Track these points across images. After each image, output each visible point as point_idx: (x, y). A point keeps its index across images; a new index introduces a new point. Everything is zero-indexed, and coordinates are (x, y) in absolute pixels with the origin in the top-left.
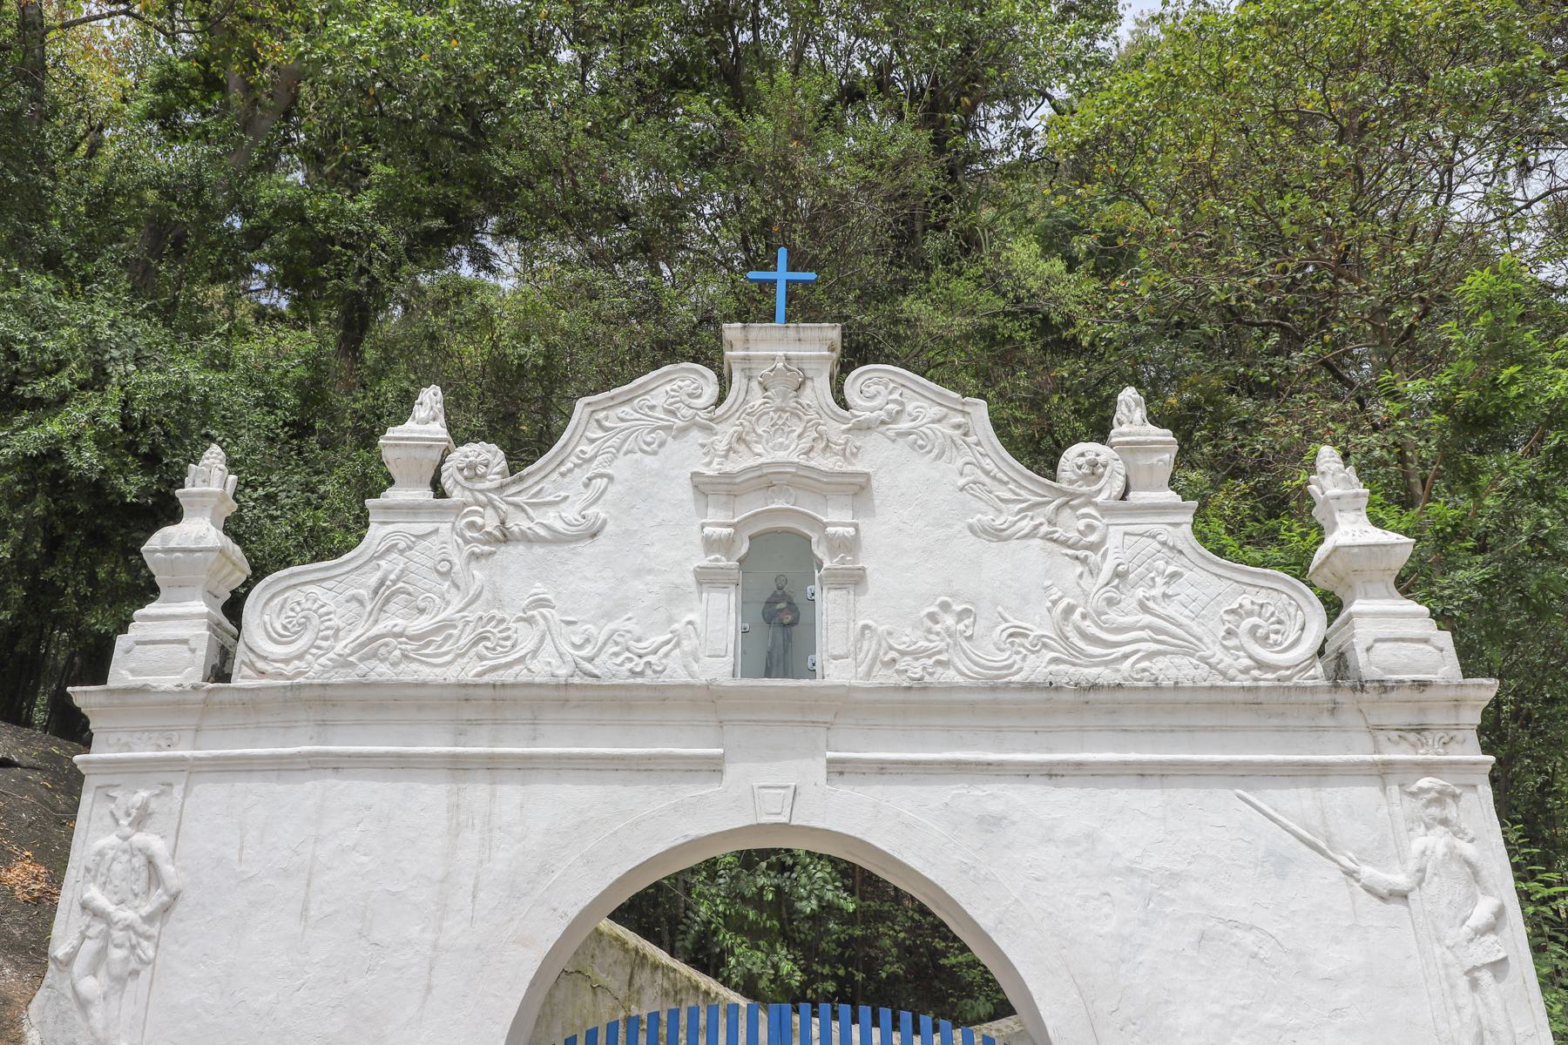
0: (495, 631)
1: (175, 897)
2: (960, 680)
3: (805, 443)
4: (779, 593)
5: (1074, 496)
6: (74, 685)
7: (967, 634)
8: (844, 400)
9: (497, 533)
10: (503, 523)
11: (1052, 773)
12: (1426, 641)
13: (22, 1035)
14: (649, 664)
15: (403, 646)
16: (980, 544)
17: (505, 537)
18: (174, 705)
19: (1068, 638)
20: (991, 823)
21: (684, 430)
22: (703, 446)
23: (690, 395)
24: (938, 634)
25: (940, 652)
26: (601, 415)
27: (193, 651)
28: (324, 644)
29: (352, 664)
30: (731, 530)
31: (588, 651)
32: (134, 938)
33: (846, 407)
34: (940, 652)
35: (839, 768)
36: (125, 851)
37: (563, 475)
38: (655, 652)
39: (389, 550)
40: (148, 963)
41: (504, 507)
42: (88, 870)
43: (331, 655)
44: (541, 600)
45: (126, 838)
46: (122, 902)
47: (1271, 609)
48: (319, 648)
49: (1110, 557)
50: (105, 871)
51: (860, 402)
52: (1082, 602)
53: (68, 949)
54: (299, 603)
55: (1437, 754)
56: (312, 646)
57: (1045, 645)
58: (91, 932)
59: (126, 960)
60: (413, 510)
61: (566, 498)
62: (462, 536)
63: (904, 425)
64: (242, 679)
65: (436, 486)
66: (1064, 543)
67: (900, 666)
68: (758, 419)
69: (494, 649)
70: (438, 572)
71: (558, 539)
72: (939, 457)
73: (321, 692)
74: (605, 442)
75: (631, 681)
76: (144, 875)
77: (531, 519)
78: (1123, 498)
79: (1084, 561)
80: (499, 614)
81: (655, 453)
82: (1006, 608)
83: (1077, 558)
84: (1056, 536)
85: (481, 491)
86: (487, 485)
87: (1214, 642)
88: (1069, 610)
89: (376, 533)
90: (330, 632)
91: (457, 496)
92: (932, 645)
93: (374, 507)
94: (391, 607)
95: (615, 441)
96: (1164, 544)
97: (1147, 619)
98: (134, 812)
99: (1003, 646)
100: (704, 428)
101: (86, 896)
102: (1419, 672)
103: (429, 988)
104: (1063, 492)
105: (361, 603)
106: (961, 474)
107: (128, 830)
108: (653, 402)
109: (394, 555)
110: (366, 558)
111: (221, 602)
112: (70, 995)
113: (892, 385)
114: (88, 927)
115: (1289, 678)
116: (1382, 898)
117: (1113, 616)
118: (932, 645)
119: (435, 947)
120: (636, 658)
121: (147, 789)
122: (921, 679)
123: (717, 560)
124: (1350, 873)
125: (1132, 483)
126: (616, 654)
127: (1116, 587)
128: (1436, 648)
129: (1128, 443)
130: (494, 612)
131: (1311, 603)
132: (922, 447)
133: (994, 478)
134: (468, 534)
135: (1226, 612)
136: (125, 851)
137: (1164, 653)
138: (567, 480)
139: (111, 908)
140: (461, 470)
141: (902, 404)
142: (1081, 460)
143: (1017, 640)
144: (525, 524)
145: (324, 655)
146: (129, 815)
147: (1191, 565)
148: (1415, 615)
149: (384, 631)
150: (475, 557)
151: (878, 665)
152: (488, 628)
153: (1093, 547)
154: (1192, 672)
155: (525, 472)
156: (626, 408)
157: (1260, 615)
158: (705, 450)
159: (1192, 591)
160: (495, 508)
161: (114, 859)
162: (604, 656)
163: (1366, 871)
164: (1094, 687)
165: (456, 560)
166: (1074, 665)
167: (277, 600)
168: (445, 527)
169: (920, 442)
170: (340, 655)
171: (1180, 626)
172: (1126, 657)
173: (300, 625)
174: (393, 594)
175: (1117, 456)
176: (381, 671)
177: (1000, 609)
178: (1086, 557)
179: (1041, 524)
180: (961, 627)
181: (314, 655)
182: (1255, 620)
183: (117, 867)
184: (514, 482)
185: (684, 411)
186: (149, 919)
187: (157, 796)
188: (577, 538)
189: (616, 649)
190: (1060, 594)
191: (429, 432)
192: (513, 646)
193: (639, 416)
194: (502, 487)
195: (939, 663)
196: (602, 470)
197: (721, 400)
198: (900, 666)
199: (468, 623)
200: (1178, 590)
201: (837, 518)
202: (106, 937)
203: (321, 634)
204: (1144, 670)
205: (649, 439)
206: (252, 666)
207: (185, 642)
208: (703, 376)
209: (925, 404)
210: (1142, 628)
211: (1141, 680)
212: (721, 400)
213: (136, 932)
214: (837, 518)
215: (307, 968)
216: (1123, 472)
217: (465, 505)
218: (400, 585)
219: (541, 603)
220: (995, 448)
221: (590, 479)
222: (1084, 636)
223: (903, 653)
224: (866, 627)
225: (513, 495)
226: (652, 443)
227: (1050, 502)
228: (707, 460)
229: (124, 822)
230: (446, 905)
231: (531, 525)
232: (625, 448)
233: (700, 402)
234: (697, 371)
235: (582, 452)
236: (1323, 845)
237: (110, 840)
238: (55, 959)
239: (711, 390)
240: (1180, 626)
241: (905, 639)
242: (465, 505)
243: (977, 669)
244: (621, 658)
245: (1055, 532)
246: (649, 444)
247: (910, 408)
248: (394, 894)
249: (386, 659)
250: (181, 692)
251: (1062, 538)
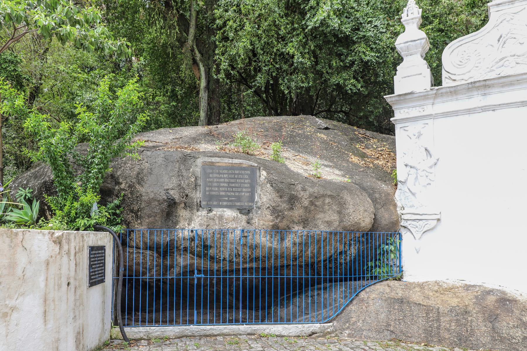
13: (396, 203)
18: (424, 97)
73: (484, 83)
93: (491, 6)
114: (410, 171)
186: (431, 167)
202: (417, 173)
250: (426, 92)
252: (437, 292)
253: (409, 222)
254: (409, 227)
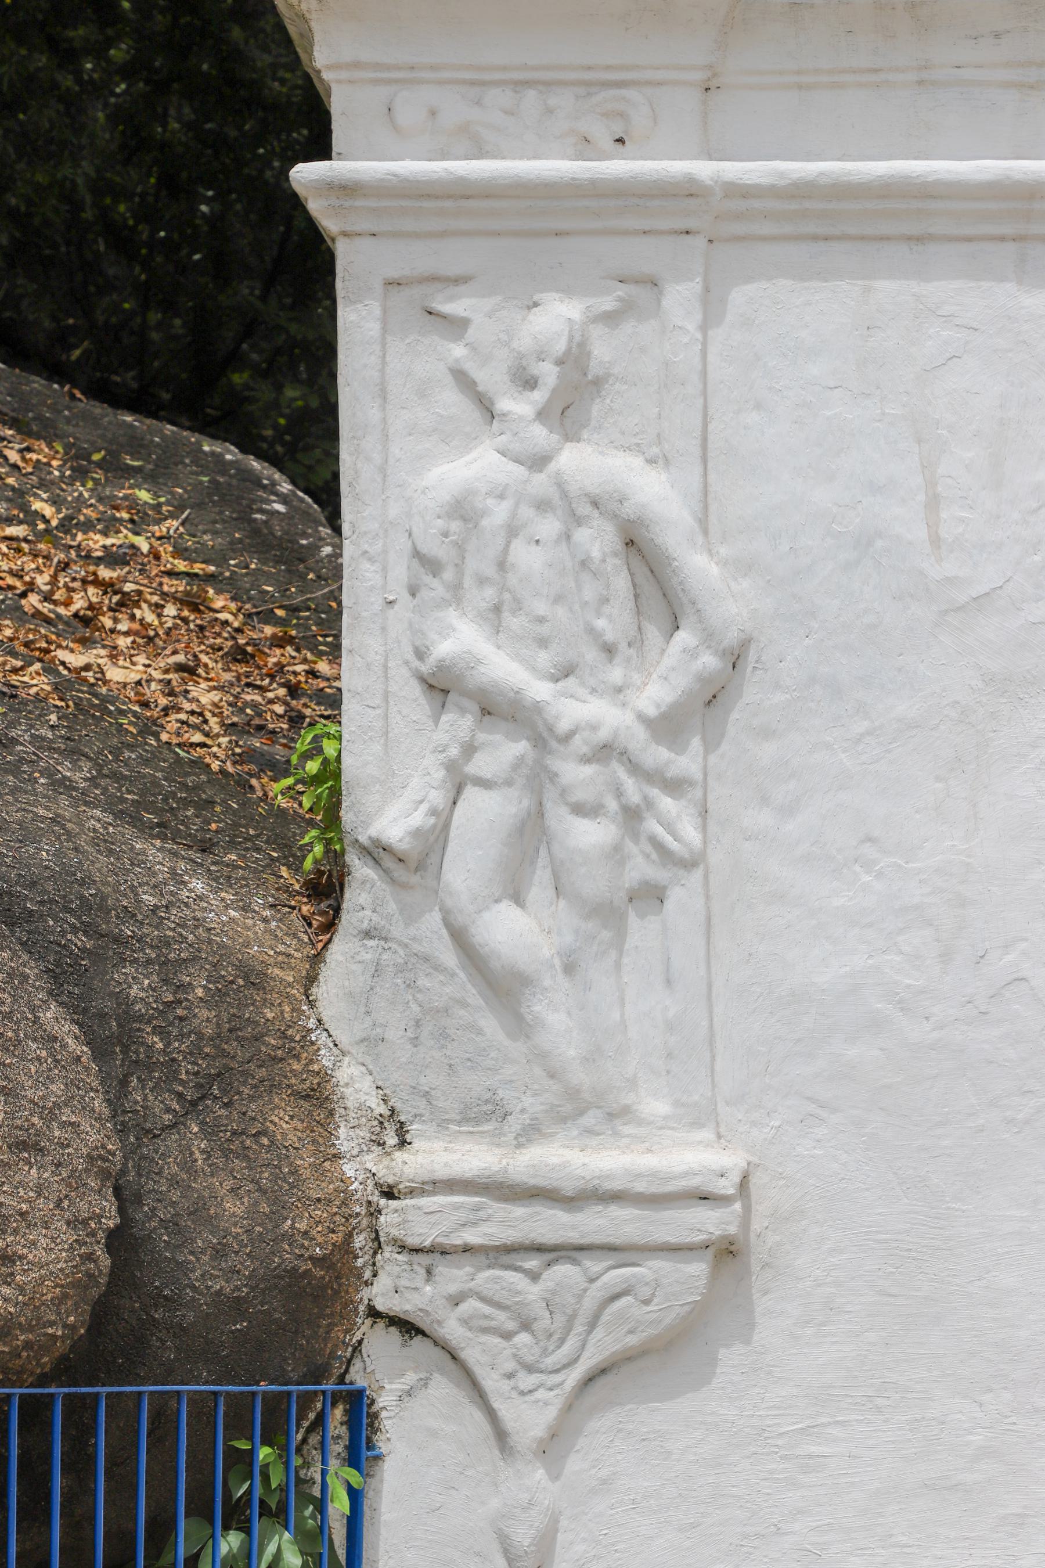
32: (633, 790)
36: (542, 506)
40: (689, 863)
42: (431, 565)
45: (538, 462)
46: (565, 672)
50: (490, 571)
53: (418, 818)
58: (482, 765)
59: (616, 854)
76: (621, 583)
98: (548, 373)
101: (444, 649)
107: (540, 435)
112: (449, 957)
121: (568, 292)
136: (542, 506)
139: (539, 690)
146: (530, 383)
161: (512, 531)
187: (610, 319)
213: (635, 768)
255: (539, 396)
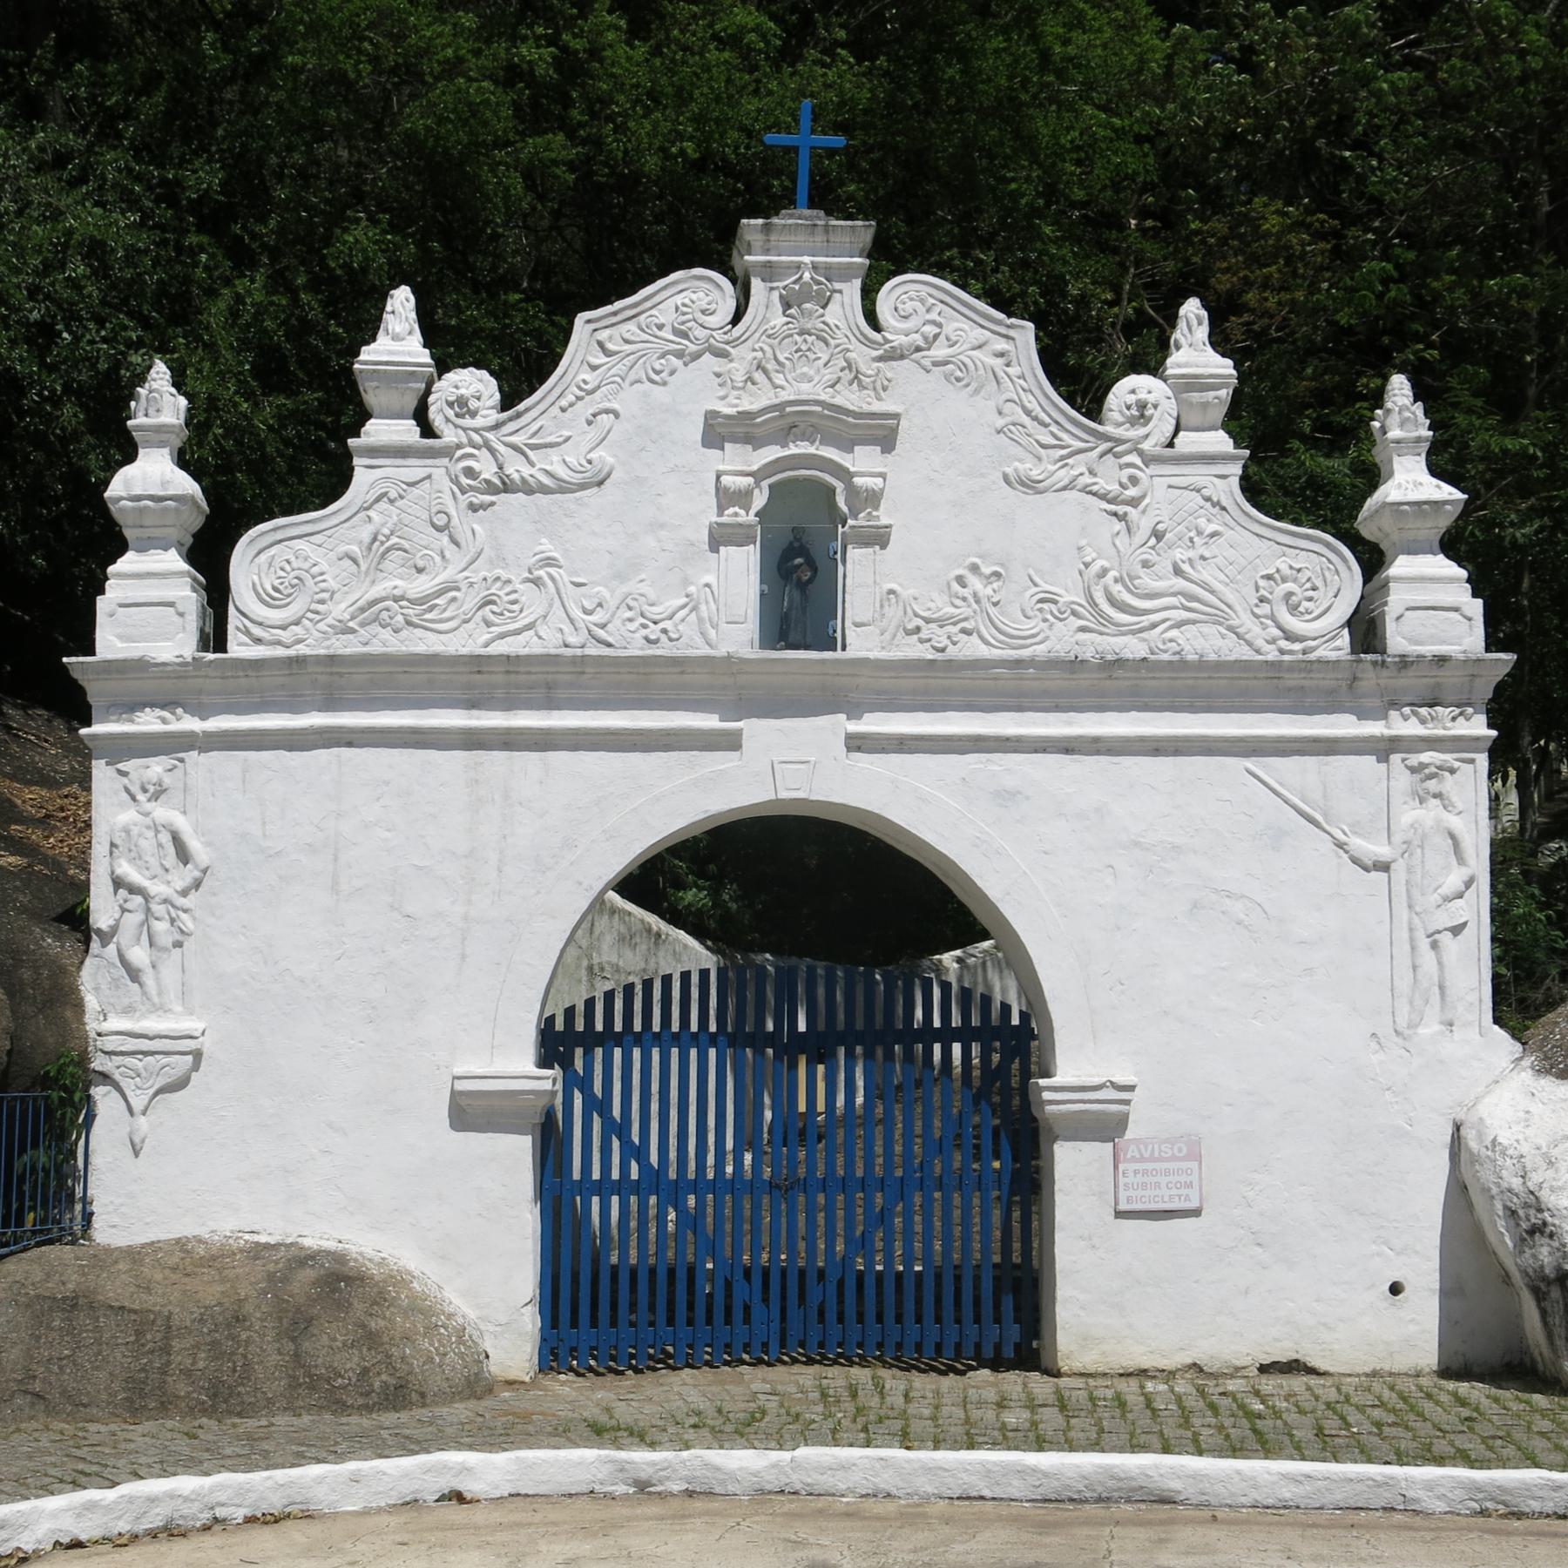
0: (501, 593)
1: (205, 871)
2: (984, 652)
3: (829, 375)
4: (796, 544)
5: (1120, 441)
6: (68, 656)
7: (994, 600)
8: (874, 311)
9: (497, 481)
10: (501, 468)
11: (1068, 747)
12: (1456, 610)
14: (665, 631)
15: (404, 611)
16: (1013, 496)
17: (507, 487)
19: (1097, 605)
20: (1006, 797)
21: (696, 356)
22: (718, 375)
23: (703, 312)
24: (964, 599)
25: (966, 619)
26: (603, 335)
27: (181, 615)
28: (320, 607)
29: (353, 631)
30: (750, 480)
31: (598, 617)
33: (876, 327)
34: (966, 619)
35: (858, 743)
36: (148, 827)
37: (563, 410)
38: (670, 618)
39: (378, 500)
41: (501, 448)
43: (330, 620)
44: (549, 558)
46: (154, 877)
47: (1308, 574)
48: (317, 613)
49: (1150, 512)
51: (893, 322)
52: (1116, 564)
53: (112, 922)
54: (288, 562)
55: (1445, 728)
56: (309, 610)
57: (1074, 613)
60: (401, 452)
61: (568, 439)
62: (457, 482)
63: (939, 352)
64: (238, 647)
65: (421, 415)
66: (1103, 497)
67: (924, 634)
68: (780, 343)
69: (502, 614)
70: (434, 525)
71: (564, 488)
72: (977, 391)
74: (610, 369)
75: (649, 652)
77: (532, 464)
78: (1171, 445)
79: (1121, 518)
80: (504, 575)
81: (665, 384)
82: (1037, 571)
83: (1115, 514)
84: (1095, 488)
85: (476, 430)
86: (478, 422)
87: (1245, 610)
88: (1104, 572)
89: (364, 478)
90: (325, 595)
91: (449, 436)
92: (957, 611)
94: (387, 565)
95: (620, 368)
96: (1208, 499)
97: (1181, 583)
99: (1030, 613)
100: (721, 354)
101: (119, 871)
102: (1443, 642)
103: (463, 957)
104: (1106, 437)
105: (355, 561)
106: (1000, 413)
108: (662, 320)
109: (383, 505)
110: (354, 510)
111: (185, 549)
113: (932, 301)
115: (1314, 649)
116: (1366, 869)
117: (1147, 581)
118: (957, 611)
119: (466, 918)
120: (651, 624)
122: (943, 650)
123: (736, 514)
124: (1340, 845)
125: (1183, 422)
126: (631, 620)
127: (1153, 548)
128: (1465, 617)
129: (1183, 376)
130: (499, 572)
131: (1349, 568)
132: (958, 380)
133: (1035, 419)
134: (465, 481)
135: (1262, 577)
137: (1194, 622)
138: (567, 414)
140: (450, 404)
141: (940, 325)
142: (1132, 399)
143: (1045, 606)
144: (526, 471)
145: (321, 620)
147: (1233, 524)
148: (1452, 580)
149: (384, 594)
150: (474, 508)
151: (901, 633)
152: (492, 591)
153: (1134, 502)
154: (1219, 642)
155: (521, 407)
156: (631, 326)
157: (1295, 580)
158: (719, 380)
159: (1230, 553)
160: (492, 451)
162: (617, 622)
163: (1358, 844)
164: (1120, 663)
165: (453, 512)
166: (1101, 634)
167: (263, 557)
168: (438, 474)
169: (959, 374)
170: (340, 621)
171: (1212, 592)
172: (1154, 626)
173: (293, 587)
174: (388, 550)
175: (1170, 394)
176: (384, 642)
177: (1032, 572)
178: (1126, 514)
179: (1081, 474)
180: (989, 591)
181: (311, 620)
182: (1290, 586)
183: (143, 843)
184: (511, 419)
185: (700, 333)
186: (184, 893)
188: (583, 486)
189: (629, 614)
190: (1094, 555)
191: (409, 354)
192: (521, 611)
193: (647, 337)
194: (497, 426)
195: (964, 631)
196: (608, 405)
197: (736, 320)
198: (924, 634)
199: (471, 585)
200: (1216, 552)
201: (863, 462)
203: (317, 597)
204: (1171, 641)
205: (658, 367)
206: (247, 633)
207: (171, 604)
208: (718, 286)
209: (966, 325)
210: (1174, 594)
211: (1165, 651)
212: (736, 320)
213: (174, 906)
214: (863, 462)
215: (344, 939)
216: (1175, 415)
217: (459, 446)
218: (394, 540)
219: (550, 562)
220: (1032, 369)
221: (594, 415)
222: (1113, 601)
223: (928, 621)
224: (891, 592)
225: (511, 434)
226: (661, 372)
227: (1092, 449)
228: (722, 393)
229: (141, 797)
230: (473, 879)
231: (533, 471)
232: (632, 376)
233: (713, 321)
234: (710, 280)
235: (585, 382)
236: (1319, 818)
237: (128, 816)
238: (99, 932)
239: (730, 305)
240: (1212, 592)
241: (932, 605)
242: (459, 446)
243: (1002, 638)
244: (636, 624)
245: (1095, 484)
246: (658, 373)
247: (949, 329)
248: (421, 868)
249: (389, 625)
251: (1102, 491)
252: (174, 1269)
253: (118, 1060)
254: (117, 1077)
255: (148, 795)
